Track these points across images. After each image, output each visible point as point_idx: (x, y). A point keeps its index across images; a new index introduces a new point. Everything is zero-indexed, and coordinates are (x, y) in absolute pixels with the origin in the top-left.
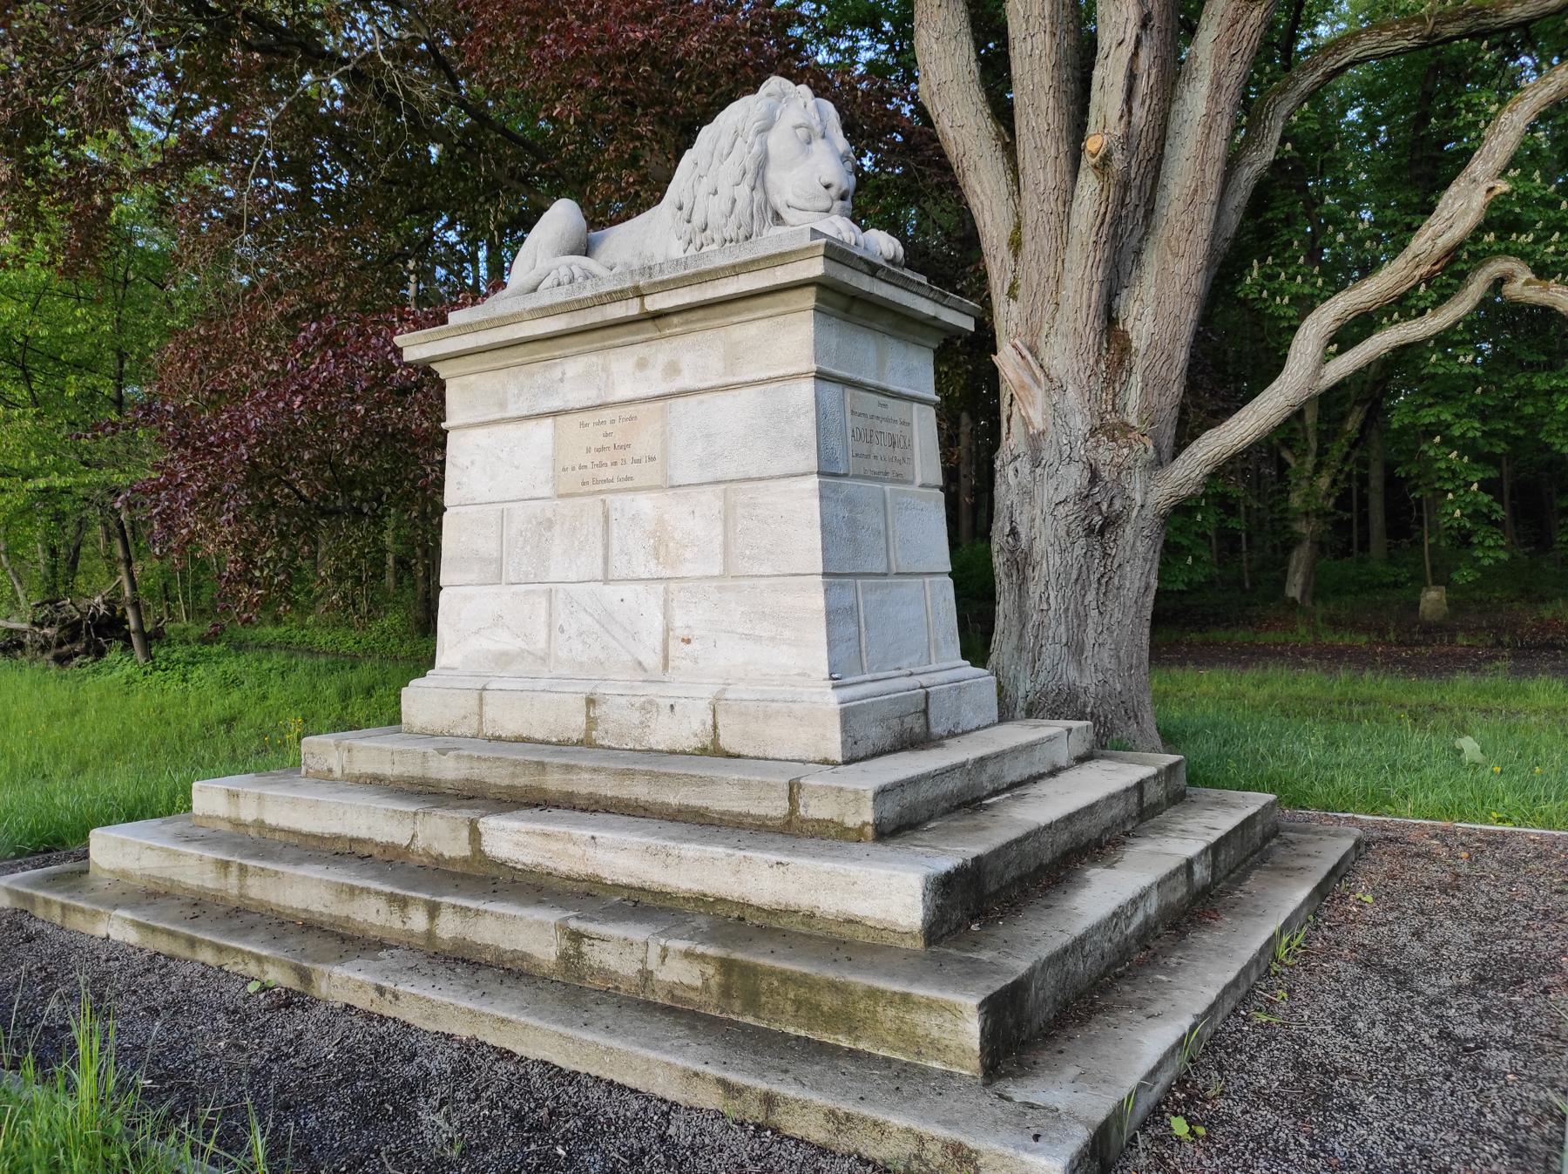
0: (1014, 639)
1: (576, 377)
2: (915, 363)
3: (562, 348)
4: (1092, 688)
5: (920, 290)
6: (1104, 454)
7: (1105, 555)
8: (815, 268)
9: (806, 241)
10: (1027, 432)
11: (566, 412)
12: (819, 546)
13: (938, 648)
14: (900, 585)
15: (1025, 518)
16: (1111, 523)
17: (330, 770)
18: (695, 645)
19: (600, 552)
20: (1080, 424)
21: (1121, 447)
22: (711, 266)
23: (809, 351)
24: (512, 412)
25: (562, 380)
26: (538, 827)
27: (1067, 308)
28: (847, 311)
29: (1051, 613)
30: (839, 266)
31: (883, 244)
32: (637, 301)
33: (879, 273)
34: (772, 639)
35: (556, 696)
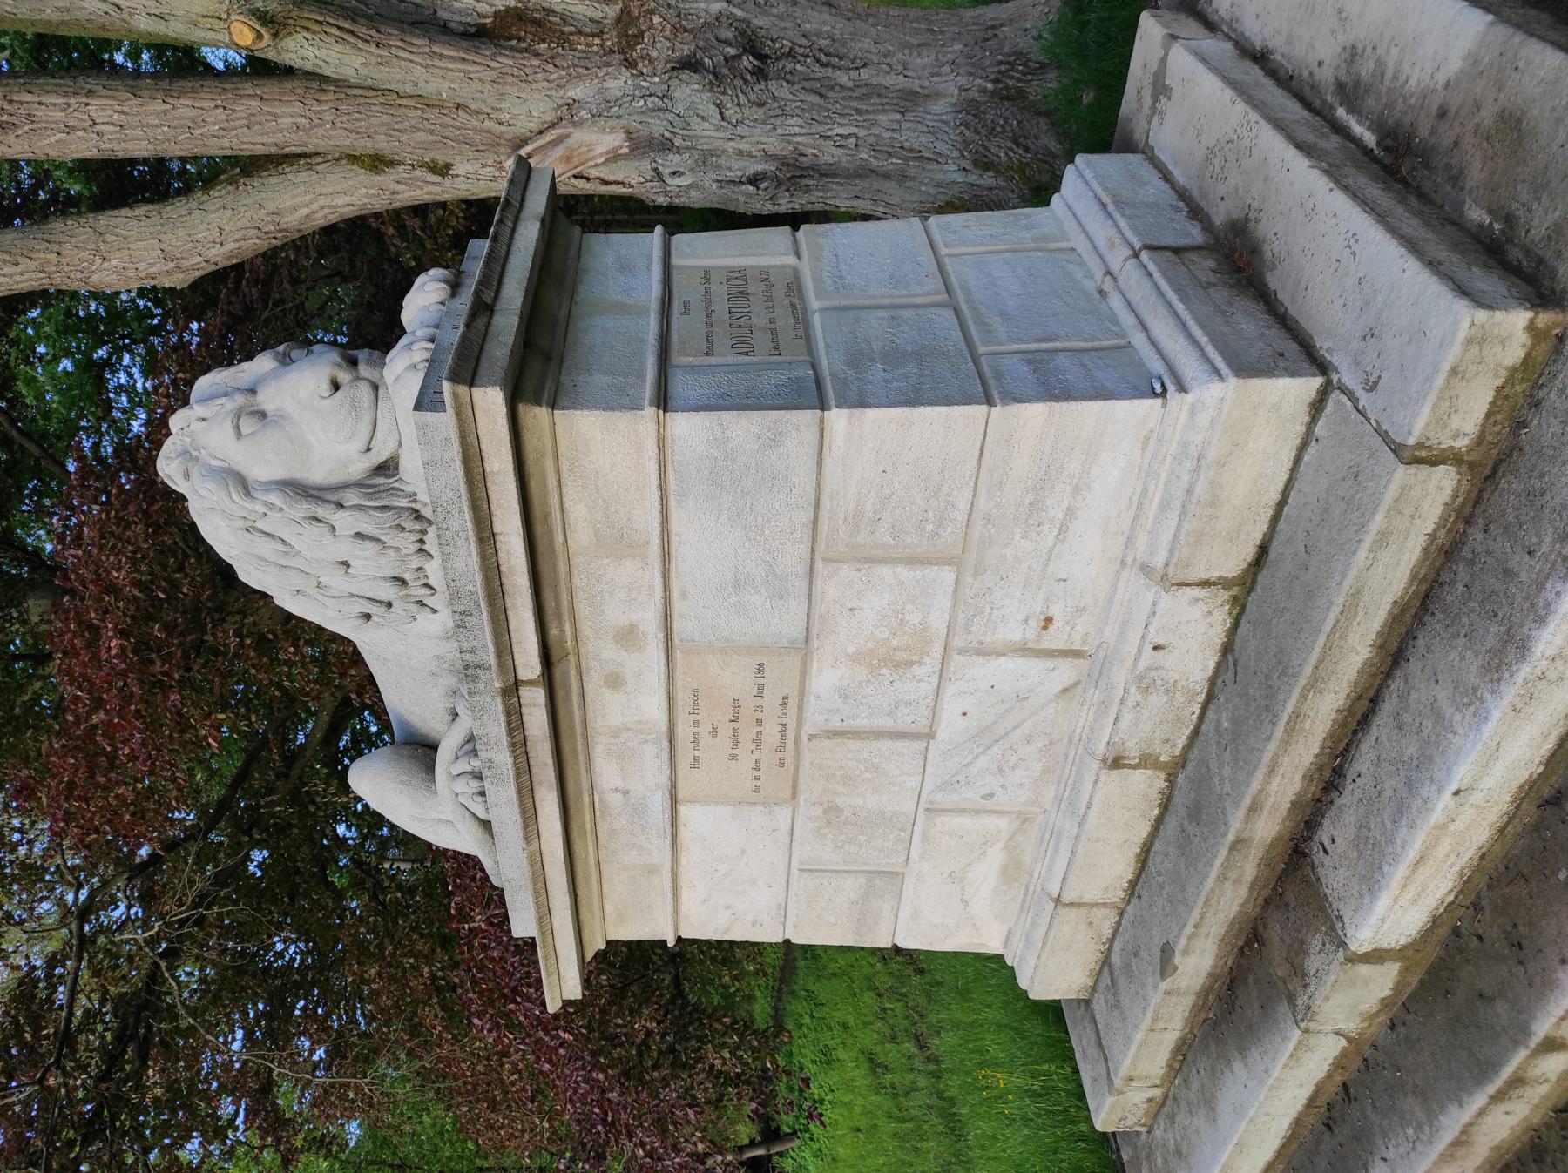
0: (888, 186)
1: (622, 774)
2: (609, 260)
3: (581, 794)
4: (962, 80)
5: (504, 238)
6: (661, 49)
7: (791, 55)
8: (490, 401)
9: (445, 422)
10: (625, 157)
11: (673, 786)
12: (944, 409)
13: (1045, 238)
14: (966, 290)
15: (736, 165)
16: (750, 44)
17: (1150, 1100)
18: (1057, 612)
19: (885, 745)
20: (618, 82)
21: (652, 26)
22: (478, 577)
23: (622, 419)
24: (663, 857)
25: (625, 793)
26: (1402, 871)
27: (465, 92)
28: (547, 357)
29: (862, 133)
30: (484, 363)
31: (424, 299)
32: (525, 692)
33: (488, 297)
34: (1077, 490)
35: (1095, 809)
